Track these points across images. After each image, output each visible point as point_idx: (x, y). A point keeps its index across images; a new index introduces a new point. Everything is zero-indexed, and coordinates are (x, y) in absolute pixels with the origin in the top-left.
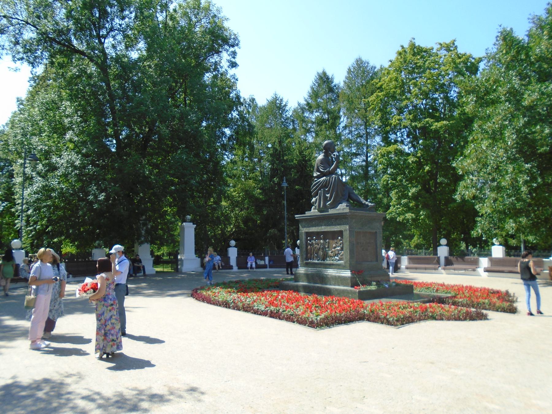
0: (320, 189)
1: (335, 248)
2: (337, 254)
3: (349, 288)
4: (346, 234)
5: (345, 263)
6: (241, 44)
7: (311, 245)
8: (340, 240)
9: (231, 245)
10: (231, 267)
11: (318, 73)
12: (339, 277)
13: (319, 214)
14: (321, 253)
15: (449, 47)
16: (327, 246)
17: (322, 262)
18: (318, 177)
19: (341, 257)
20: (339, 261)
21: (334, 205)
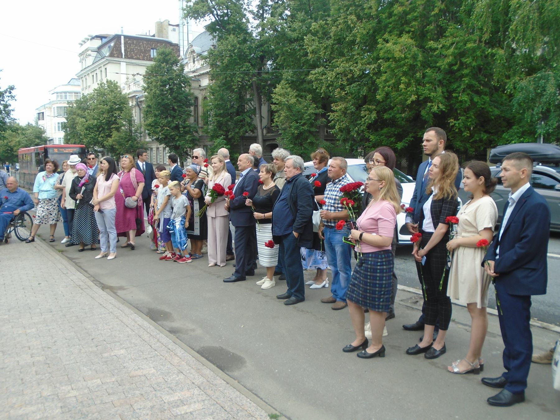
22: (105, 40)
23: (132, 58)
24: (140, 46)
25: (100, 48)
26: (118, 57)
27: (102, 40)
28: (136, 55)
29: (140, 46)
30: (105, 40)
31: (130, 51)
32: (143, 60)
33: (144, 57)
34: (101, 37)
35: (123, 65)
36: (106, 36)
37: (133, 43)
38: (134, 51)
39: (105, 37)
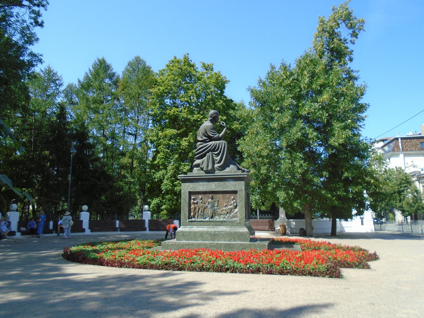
0: (208, 152)
1: (226, 206)
2: (230, 212)
3: (248, 243)
4: (242, 194)
5: (240, 220)
6: (48, 7)
7: (194, 203)
8: (233, 199)
9: (12, 209)
10: (83, 230)
11: (98, 59)
12: (236, 233)
13: (205, 174)
14: (209, 211)
15: (208, 68)
16: (216, 205)
17: (211, 219)
18: (204, 141)
19: (235, 215)
20: (232, 218)
21: (222, 168)
22: (386, 142)
23: (407, 150)
24: (412, 142)
25: (383, 147)
26: (397, 151)
27: (384, 142)
28: (410, 148)
29: (412, 142)
30: (386, 142)
31: (406, 146)
32: (415, 150)
33: (415, 148)
34: (383, 140)
35: (402, 156)
36: (386, 139)
37: (407, 142)
38: (408, 146)
39: (386, 140)
